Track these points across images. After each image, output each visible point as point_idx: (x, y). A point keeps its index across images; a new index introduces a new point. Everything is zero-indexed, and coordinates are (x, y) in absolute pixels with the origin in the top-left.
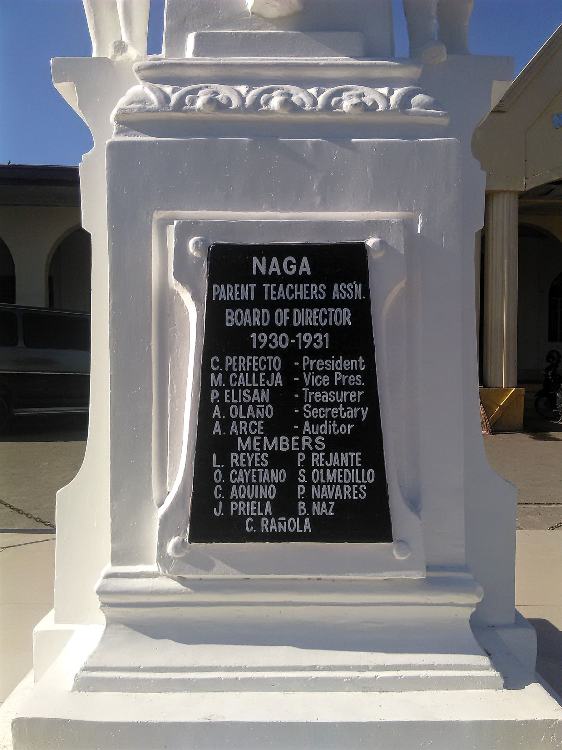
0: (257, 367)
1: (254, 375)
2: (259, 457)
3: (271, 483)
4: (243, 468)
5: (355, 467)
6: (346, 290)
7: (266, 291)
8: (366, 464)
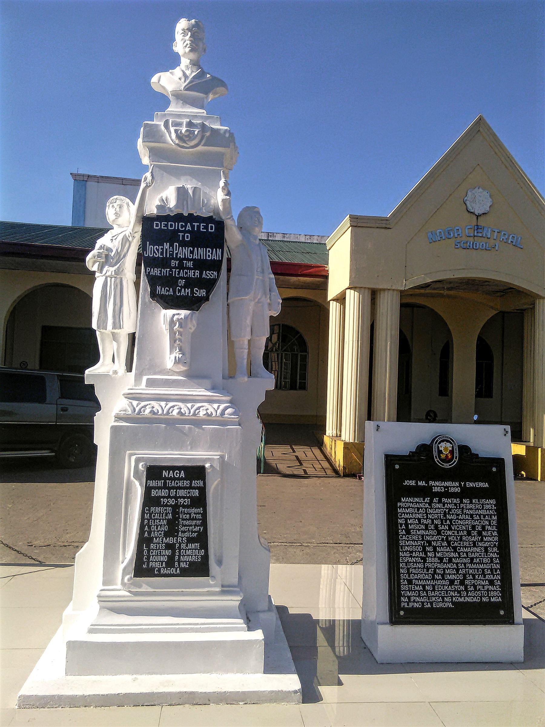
0: (163, 511)
1: (161, 514)
2: (162, 545)
3: (165, 555)
4: (155, 550)
5: (197, 549)
6: (197, 483)
7: (168, 483)
8: (201, 548)
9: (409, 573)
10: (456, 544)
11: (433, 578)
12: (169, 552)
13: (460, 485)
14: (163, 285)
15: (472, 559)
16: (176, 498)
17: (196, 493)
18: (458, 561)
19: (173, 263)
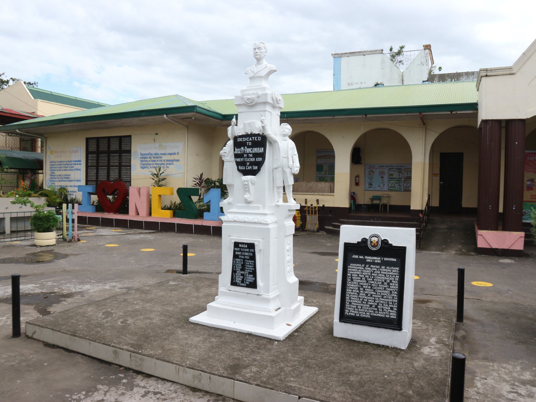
9: (350, 299)
10: (375, 288)
11: (362, 303)
12: (242, 277)
13: (381, 259)
14: (241, 166)
15: (383, 296)
16: (244, 256)
17: (251, 254)
18: (375, 296)
19: (245, 155)
